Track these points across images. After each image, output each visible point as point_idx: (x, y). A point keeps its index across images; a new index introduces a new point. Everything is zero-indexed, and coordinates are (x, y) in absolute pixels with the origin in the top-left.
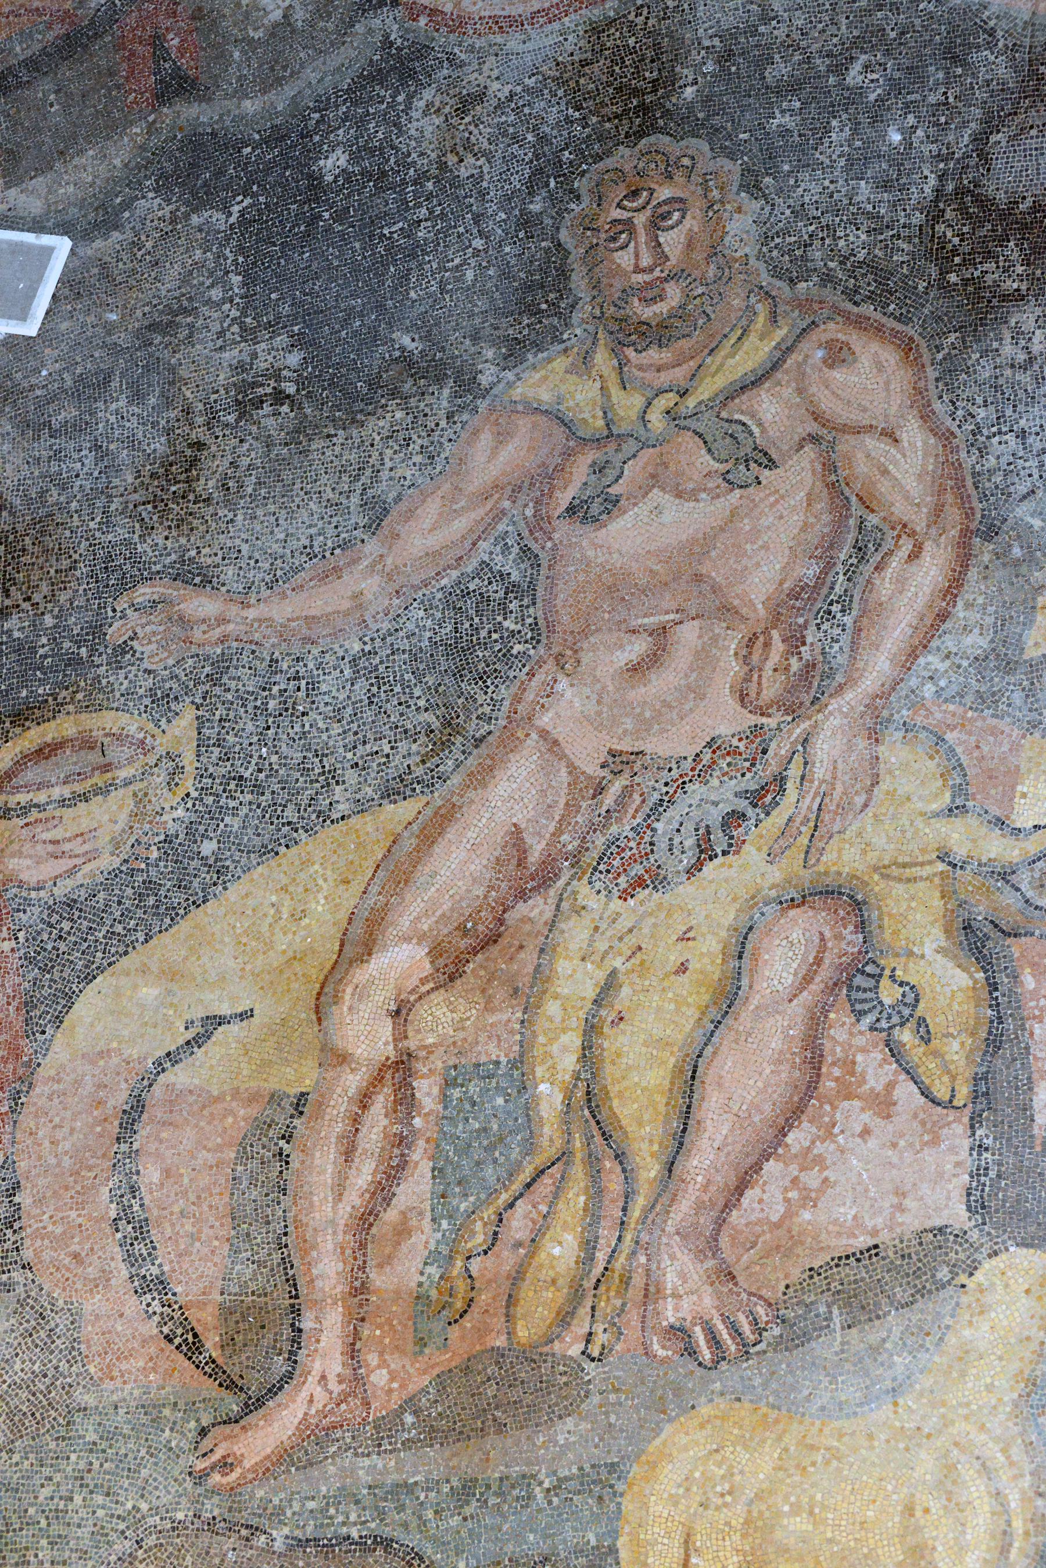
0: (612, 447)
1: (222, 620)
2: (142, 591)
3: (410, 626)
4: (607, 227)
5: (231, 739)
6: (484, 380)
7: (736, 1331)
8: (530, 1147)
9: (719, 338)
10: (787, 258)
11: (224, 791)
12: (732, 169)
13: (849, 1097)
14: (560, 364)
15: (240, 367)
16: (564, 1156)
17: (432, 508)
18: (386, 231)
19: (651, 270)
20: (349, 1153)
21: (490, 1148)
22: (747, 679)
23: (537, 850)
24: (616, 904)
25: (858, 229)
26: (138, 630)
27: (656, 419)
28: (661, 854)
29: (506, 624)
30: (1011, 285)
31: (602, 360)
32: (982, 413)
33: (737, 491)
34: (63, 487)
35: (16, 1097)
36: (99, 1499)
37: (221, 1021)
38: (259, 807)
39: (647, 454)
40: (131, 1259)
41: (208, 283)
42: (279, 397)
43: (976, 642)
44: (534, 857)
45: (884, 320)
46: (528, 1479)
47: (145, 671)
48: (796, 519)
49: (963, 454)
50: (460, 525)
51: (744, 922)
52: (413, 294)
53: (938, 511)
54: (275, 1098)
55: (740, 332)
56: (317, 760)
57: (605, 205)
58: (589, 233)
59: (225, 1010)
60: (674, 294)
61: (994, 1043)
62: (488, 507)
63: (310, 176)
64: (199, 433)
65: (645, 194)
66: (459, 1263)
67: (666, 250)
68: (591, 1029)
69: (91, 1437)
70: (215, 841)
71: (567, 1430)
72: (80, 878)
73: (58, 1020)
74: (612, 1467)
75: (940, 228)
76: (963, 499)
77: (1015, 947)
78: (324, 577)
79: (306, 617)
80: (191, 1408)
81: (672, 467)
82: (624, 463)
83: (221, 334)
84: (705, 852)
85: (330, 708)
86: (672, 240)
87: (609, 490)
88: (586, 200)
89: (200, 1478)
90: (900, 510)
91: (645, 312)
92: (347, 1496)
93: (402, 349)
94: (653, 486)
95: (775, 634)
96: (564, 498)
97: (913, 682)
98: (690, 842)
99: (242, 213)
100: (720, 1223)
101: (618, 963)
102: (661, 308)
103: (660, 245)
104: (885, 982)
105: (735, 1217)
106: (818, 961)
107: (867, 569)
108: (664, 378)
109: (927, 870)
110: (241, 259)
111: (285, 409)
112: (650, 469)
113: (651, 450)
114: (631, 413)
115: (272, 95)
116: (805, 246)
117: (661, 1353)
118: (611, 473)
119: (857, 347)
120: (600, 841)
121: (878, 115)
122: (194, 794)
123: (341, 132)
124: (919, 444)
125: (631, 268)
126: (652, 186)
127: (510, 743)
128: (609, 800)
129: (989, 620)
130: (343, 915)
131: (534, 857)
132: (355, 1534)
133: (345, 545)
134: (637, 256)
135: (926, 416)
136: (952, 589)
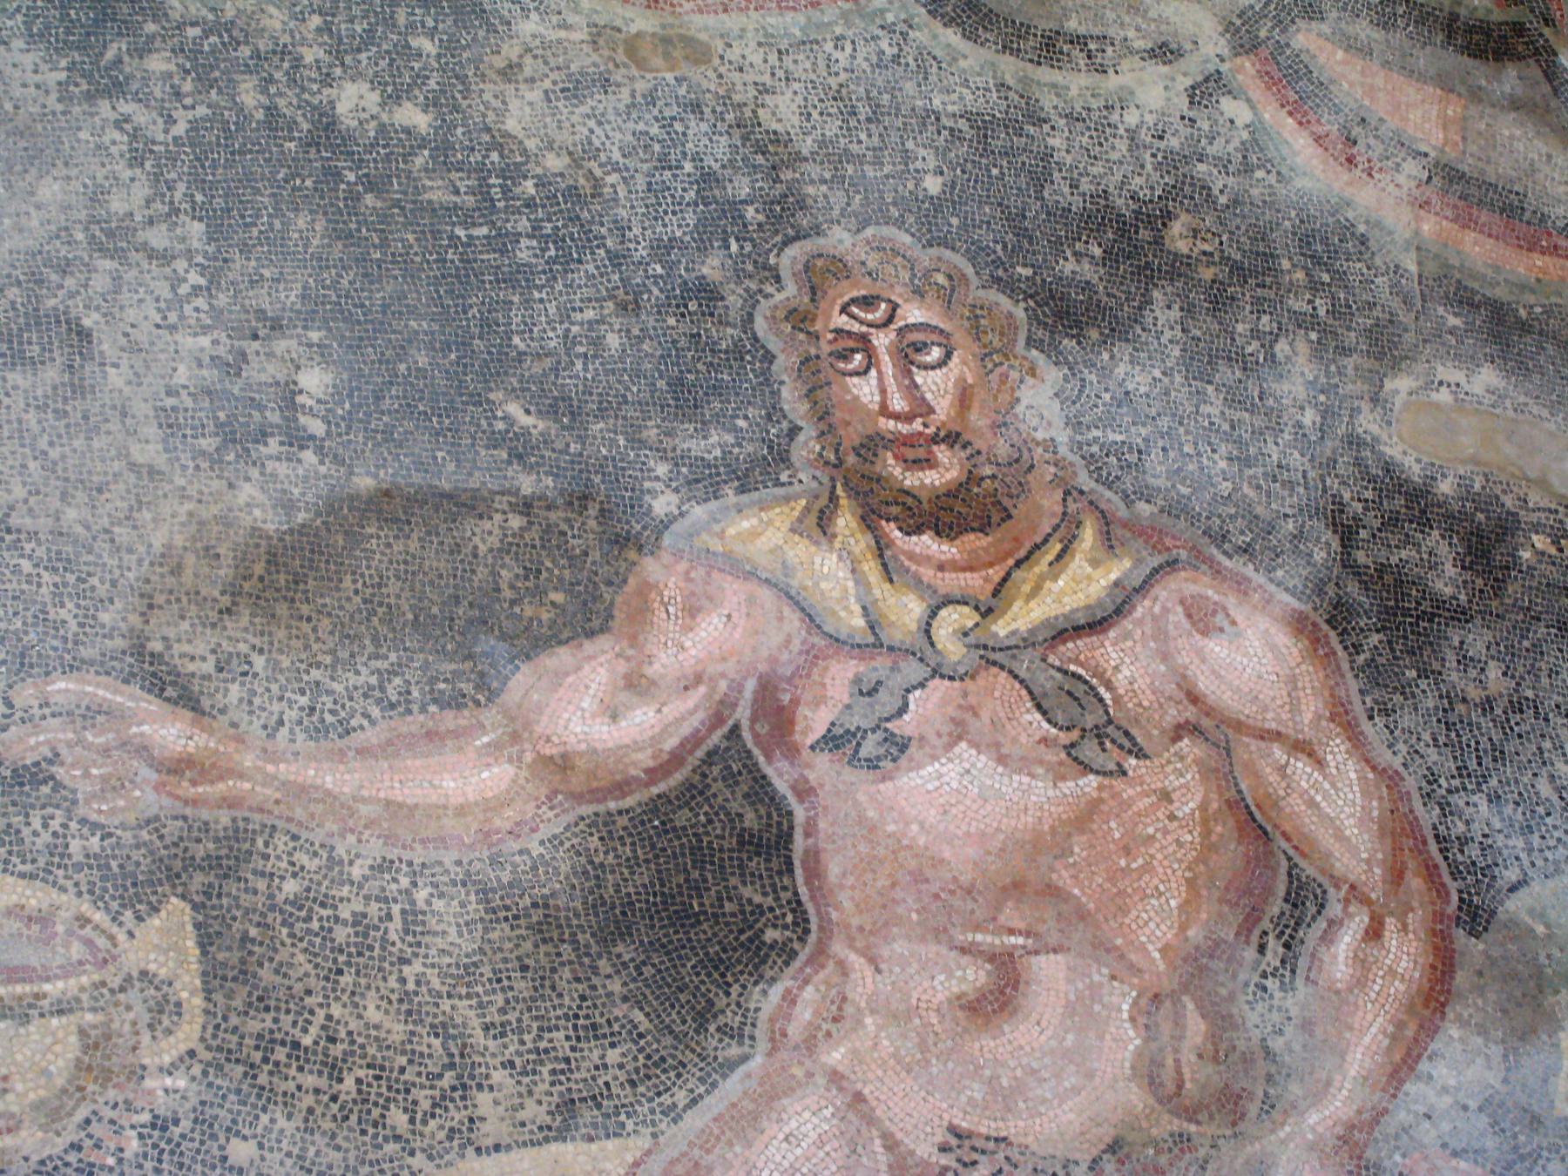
0: (882, 663)
2: (61, 685)
4: (830, 336)
9: (1027, 546)
10: (1113, 460)
11: (266, 1060)
18: (460, 232)
19: (908, 418)
25: (1214, 451)
26: (64, 751)
29: (747, 892)
33: (1091, 777)
38: (334, 1098)
39: (939, 686)
45: (1272, 588)
47: (83, 821)
49: (1417, 804)
52: (516, 340)
53: (1396, 876)
55: (1059, 547)
56: (436, 1042)
57: (823, 305)
58: (802, 336)
62: (691, 704)
65: (883, 306)
67: (929, 396)
70: (253, 1143)
76: (1431, 872)
79: (388, 803)
81: (985, 716)
82: (908, 691)
86: (937, 385)
87: (889, 725)
88: (791, 289)
91: (911, 480)
94: (960, 738)
97: (1403, 1116)
99: (194, 125)
102: (931, 478)
103: (916, 386)
108: (953, 582)
110: (199, 198)
111: (309, 456)
112: (951, 711)
113: (947, 683)
114: (907, 619)
116: (1140, 452)
118: (886, 701)
119: (1238, 614)
122: (207, 1056)
123: (363, 56)
124: (1353, 775)
125: (877, 407)
126: (893, 298)
134: (883, 392)
135: (1355, 738)
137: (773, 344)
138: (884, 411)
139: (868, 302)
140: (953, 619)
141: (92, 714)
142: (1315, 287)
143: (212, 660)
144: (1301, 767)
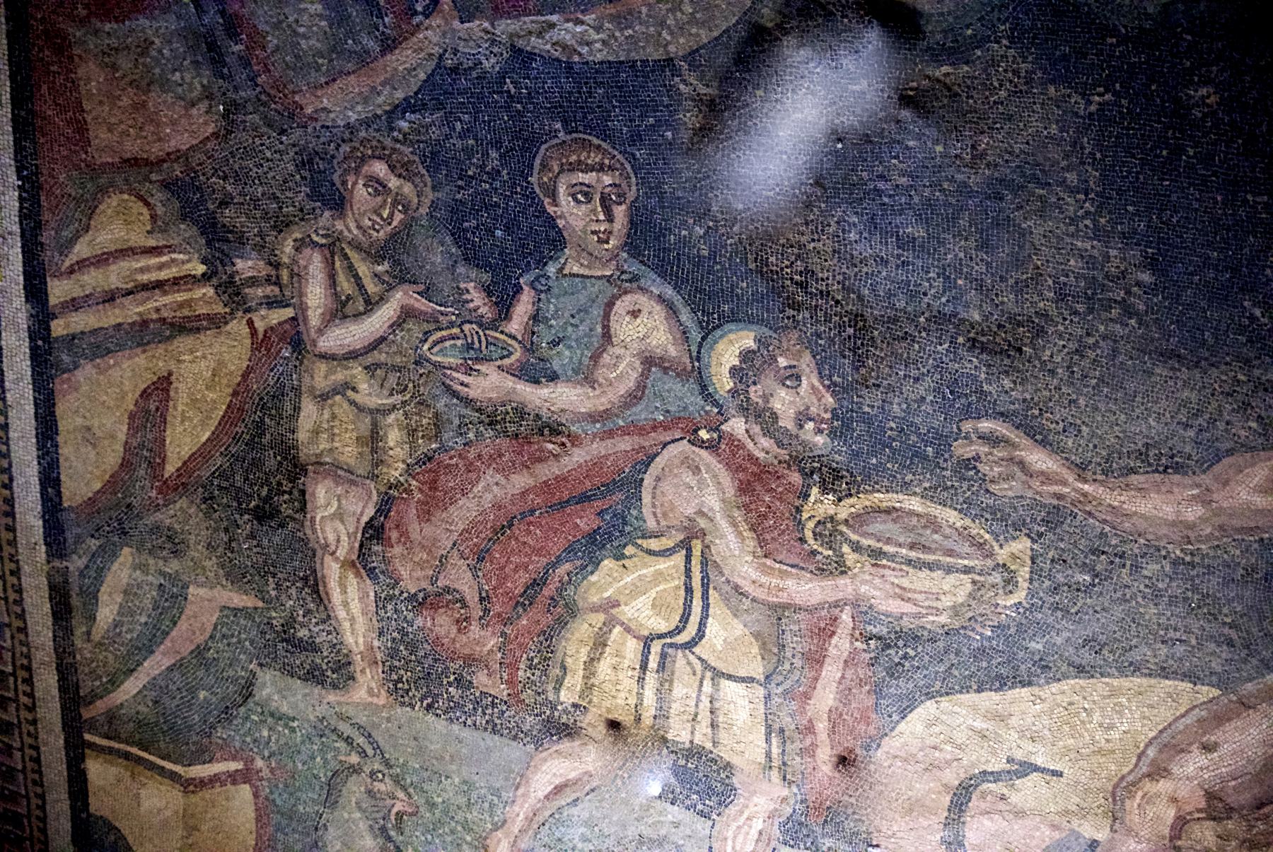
41: (1064, 163)
59: (1039, 761)
85: (1147, 590)
93: (1252, 318)
110: (1098, 156)
143: (1061, 425)
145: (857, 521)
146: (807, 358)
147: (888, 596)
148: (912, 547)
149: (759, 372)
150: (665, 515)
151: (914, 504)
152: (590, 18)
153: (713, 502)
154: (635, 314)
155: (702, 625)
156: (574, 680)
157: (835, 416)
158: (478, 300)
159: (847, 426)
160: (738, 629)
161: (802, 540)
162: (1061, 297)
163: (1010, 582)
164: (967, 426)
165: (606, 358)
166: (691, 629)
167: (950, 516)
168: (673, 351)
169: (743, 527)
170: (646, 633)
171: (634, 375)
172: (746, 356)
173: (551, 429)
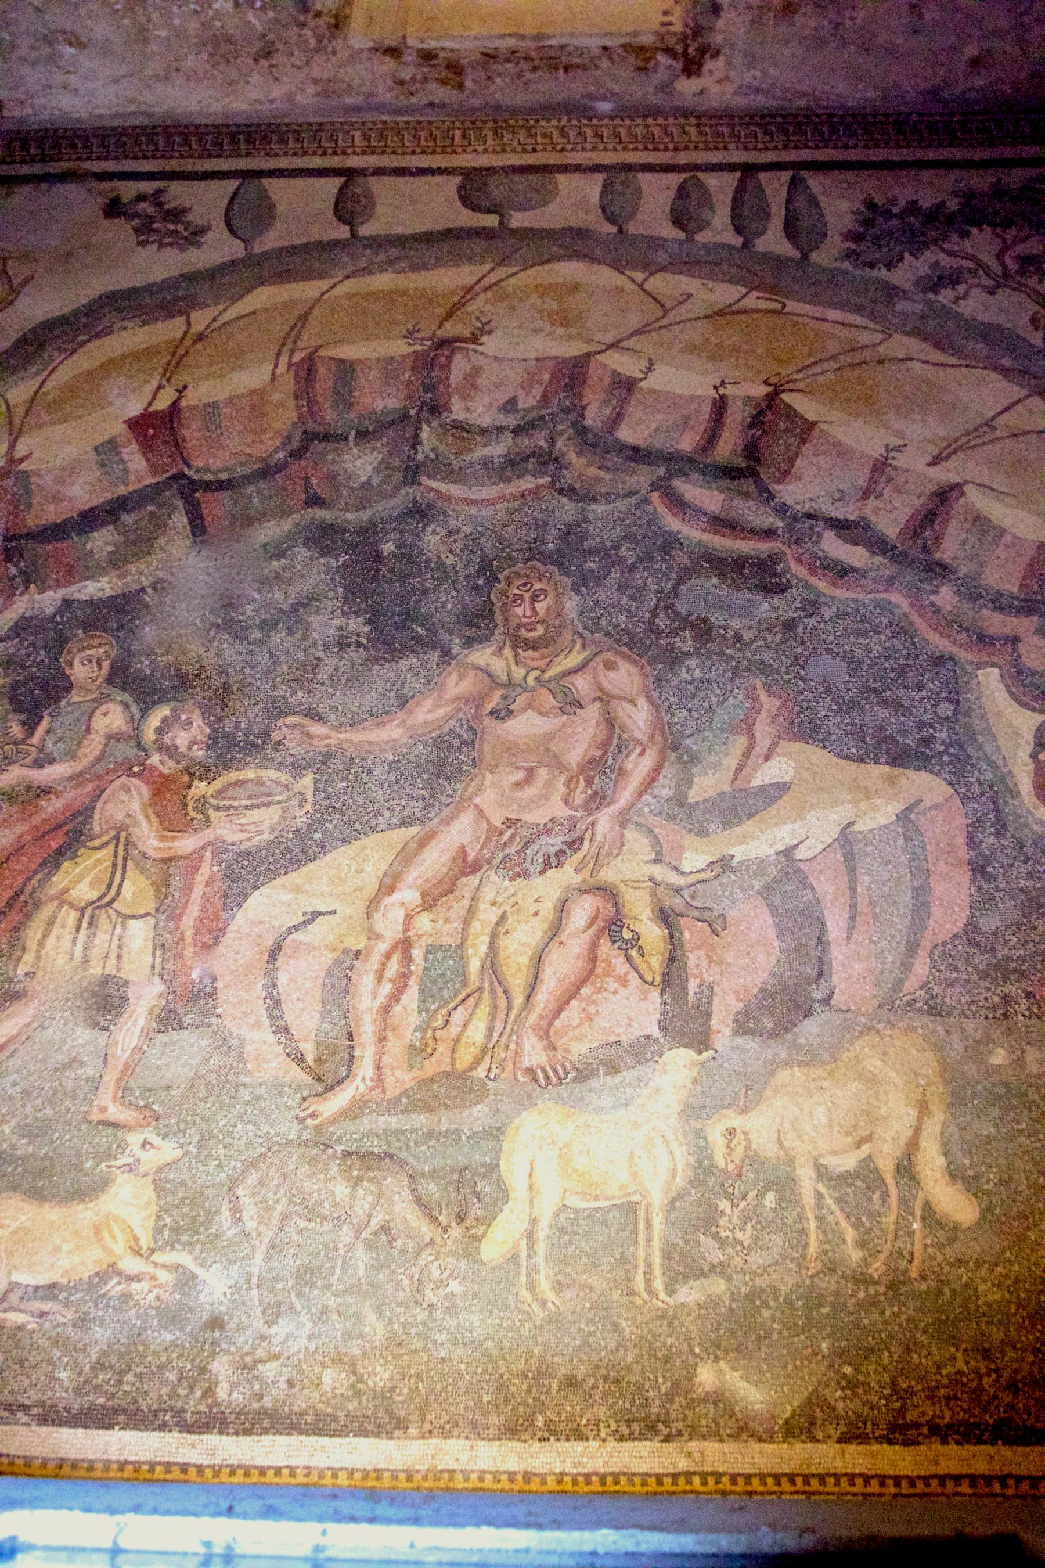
0: (510, 691)
1: (327, 737)
3: (416, 752)
5: (330, 790)
6: (454, 652)
7: (556, 1072)
8: (464, 984)
12: (568, 581)
13: (608, 976)
14: (489, 651)
15: (341, 629)
16: (480, 989)
17: (428, 703)
20: (380, 977)
21: (447, 982)
22: (569, 794)
23: (472, 856)
24: (507, 883)
27: (530, 680)
28: (527, 865)
30: (685, 649)
31: (507, 651)
32: (672, 699)
34: (252, 668)
35: (216, 938)
36: (250, 1127)
37: (320, 914)
40: (271, 1017)
42: (359, 644)
43: (667, 793)
44: (470, 859)
46: (458, 1132)
48: (591, 731)
50: (441, 712)
51: (564, 898)
53: (652, 737)
54: (346, 951)
59: (322, 909)
60: (540, 629)
61: (672, 960)
63: (377, 551)
64: (321, 654)
66: (430, 1032)
68: (494, 936)
69: (247, 1098)
71: (480, 1111)
72: (255, 842)
73: (240, 905)
74: (498, 1129)
75: (657, 621)
77: (682, 921)
78: (378, 725)
80: (299, 1088)
83: (332, 613)
84: (547, 865)
86: (541, 607)
89: (302, 1121)
90: (638, 734)
92: (370, 1134)
95: (581, 778)
96: (489, 707)
98: (541, 860)
100: (550, 1024)
101: (507, 908)
102: (534, 634)
104: (625, 930)
105: (557, 1023)
106: (596, 918)
107: (622, 756)
108: (536, 664)
109: (645, 885)
115: (361, 513)
117: (522, 1079)
118: (511, 700)
120: (501, 855)
121: (632, 569)
127: (460, 809)
128: (505, 838)
129: (673, 784)
130: (381, 873)
131: (470, 859)
132: (376, 1151)
133: (387, 713)
135: (648, 697)
136: (657, 770)
137: (495, 601)
138: (524, 616)
139: (525, 585)
140: (536, 673)
141: (295, 726)
142: (663, 560)
144: (628, 707)
145: (219, 793)
146: (197, 712)
147: (233, 832)
148: (249, 798)
149: (168, 726)
150: (107, 822)
151: (250, 774)
152: (106, 579)
153: (136, 806)
154: (105, 714)
155: (121, 885)
156: (29, 958)
157: (210, 738)
158: (17, 731)
159: (216, 742)
160: (143, 883)
161: (186, 814)
162: (327, 647)
163: (302, 802)
164: (280, 723)
165: (86, 742)
166: (113, 892)
167: (272, 774)
168: (124, 728)
169: (153, 816)
170: (83, 904)
171: (100, 747)
172: (164, 720)
173: (45, 791)
